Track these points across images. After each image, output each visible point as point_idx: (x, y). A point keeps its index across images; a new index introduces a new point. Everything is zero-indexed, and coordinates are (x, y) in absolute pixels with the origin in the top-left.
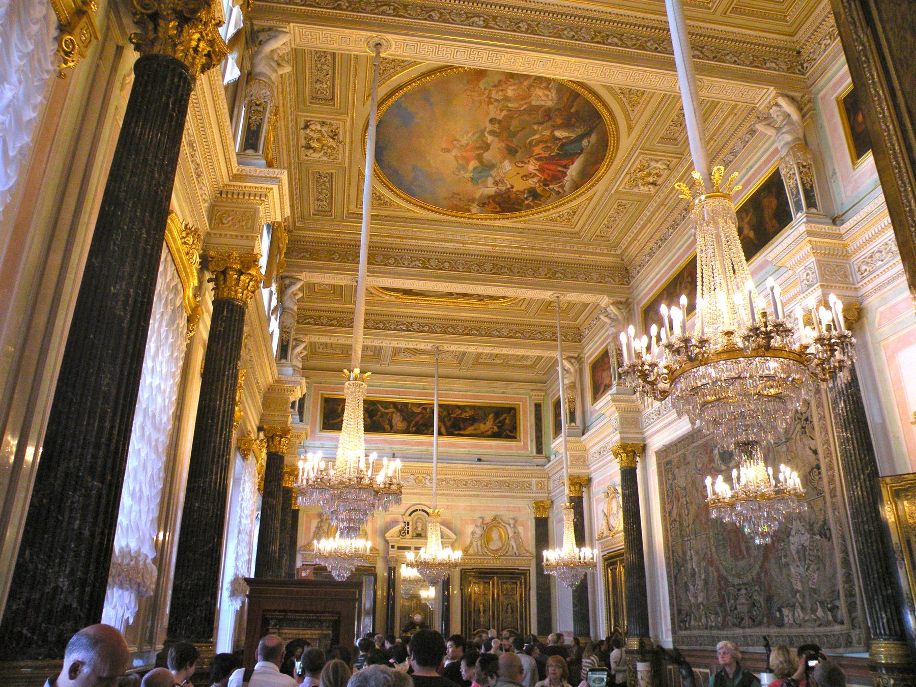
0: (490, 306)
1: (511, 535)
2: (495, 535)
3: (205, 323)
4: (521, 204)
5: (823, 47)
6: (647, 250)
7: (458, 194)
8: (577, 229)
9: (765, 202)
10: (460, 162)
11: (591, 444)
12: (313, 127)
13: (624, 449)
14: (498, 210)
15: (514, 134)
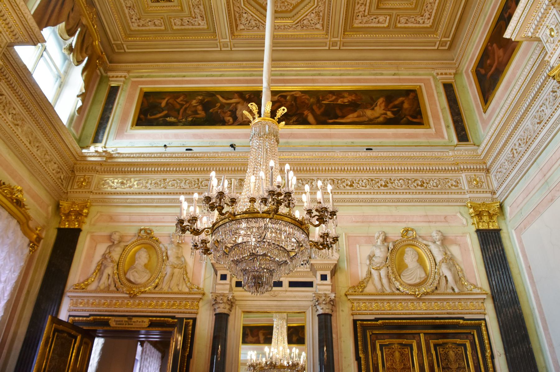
1: (439, 258)
2: (410, 259)
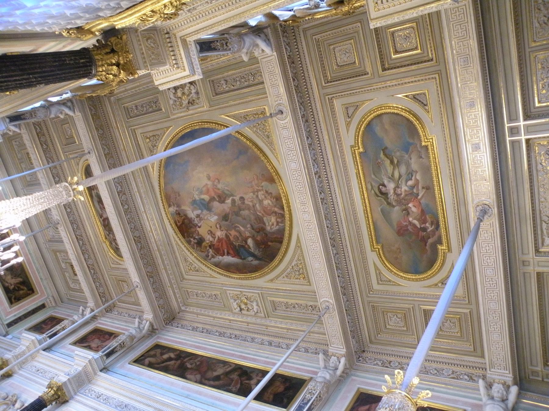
0: (104, 245)
3: (64, 47)
4: (189, 236)
5: (375, 362)
6: (196, 325)
7: (179, 195)
8: (186, 277)
9: (278, 383)
10: (204, 189)
11: (41, 360)
12: (192, 87)
13: (57, 390)
14: (179, 224)
15: (237, 214)
